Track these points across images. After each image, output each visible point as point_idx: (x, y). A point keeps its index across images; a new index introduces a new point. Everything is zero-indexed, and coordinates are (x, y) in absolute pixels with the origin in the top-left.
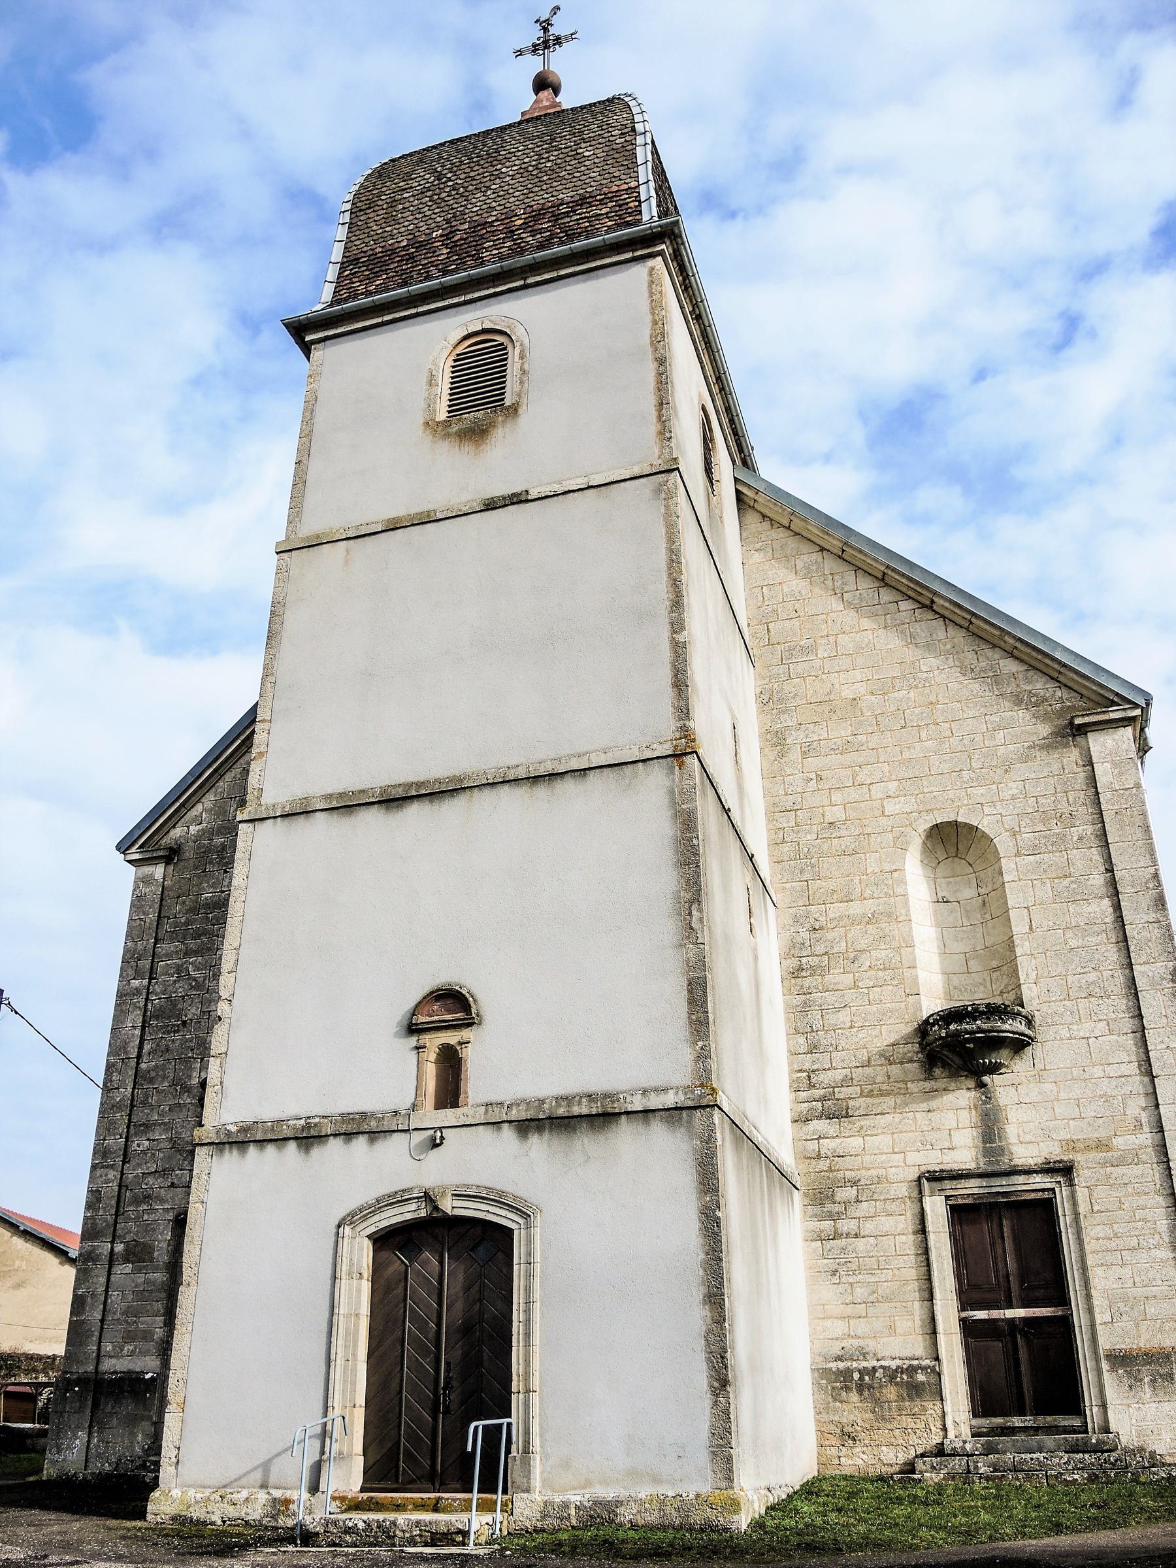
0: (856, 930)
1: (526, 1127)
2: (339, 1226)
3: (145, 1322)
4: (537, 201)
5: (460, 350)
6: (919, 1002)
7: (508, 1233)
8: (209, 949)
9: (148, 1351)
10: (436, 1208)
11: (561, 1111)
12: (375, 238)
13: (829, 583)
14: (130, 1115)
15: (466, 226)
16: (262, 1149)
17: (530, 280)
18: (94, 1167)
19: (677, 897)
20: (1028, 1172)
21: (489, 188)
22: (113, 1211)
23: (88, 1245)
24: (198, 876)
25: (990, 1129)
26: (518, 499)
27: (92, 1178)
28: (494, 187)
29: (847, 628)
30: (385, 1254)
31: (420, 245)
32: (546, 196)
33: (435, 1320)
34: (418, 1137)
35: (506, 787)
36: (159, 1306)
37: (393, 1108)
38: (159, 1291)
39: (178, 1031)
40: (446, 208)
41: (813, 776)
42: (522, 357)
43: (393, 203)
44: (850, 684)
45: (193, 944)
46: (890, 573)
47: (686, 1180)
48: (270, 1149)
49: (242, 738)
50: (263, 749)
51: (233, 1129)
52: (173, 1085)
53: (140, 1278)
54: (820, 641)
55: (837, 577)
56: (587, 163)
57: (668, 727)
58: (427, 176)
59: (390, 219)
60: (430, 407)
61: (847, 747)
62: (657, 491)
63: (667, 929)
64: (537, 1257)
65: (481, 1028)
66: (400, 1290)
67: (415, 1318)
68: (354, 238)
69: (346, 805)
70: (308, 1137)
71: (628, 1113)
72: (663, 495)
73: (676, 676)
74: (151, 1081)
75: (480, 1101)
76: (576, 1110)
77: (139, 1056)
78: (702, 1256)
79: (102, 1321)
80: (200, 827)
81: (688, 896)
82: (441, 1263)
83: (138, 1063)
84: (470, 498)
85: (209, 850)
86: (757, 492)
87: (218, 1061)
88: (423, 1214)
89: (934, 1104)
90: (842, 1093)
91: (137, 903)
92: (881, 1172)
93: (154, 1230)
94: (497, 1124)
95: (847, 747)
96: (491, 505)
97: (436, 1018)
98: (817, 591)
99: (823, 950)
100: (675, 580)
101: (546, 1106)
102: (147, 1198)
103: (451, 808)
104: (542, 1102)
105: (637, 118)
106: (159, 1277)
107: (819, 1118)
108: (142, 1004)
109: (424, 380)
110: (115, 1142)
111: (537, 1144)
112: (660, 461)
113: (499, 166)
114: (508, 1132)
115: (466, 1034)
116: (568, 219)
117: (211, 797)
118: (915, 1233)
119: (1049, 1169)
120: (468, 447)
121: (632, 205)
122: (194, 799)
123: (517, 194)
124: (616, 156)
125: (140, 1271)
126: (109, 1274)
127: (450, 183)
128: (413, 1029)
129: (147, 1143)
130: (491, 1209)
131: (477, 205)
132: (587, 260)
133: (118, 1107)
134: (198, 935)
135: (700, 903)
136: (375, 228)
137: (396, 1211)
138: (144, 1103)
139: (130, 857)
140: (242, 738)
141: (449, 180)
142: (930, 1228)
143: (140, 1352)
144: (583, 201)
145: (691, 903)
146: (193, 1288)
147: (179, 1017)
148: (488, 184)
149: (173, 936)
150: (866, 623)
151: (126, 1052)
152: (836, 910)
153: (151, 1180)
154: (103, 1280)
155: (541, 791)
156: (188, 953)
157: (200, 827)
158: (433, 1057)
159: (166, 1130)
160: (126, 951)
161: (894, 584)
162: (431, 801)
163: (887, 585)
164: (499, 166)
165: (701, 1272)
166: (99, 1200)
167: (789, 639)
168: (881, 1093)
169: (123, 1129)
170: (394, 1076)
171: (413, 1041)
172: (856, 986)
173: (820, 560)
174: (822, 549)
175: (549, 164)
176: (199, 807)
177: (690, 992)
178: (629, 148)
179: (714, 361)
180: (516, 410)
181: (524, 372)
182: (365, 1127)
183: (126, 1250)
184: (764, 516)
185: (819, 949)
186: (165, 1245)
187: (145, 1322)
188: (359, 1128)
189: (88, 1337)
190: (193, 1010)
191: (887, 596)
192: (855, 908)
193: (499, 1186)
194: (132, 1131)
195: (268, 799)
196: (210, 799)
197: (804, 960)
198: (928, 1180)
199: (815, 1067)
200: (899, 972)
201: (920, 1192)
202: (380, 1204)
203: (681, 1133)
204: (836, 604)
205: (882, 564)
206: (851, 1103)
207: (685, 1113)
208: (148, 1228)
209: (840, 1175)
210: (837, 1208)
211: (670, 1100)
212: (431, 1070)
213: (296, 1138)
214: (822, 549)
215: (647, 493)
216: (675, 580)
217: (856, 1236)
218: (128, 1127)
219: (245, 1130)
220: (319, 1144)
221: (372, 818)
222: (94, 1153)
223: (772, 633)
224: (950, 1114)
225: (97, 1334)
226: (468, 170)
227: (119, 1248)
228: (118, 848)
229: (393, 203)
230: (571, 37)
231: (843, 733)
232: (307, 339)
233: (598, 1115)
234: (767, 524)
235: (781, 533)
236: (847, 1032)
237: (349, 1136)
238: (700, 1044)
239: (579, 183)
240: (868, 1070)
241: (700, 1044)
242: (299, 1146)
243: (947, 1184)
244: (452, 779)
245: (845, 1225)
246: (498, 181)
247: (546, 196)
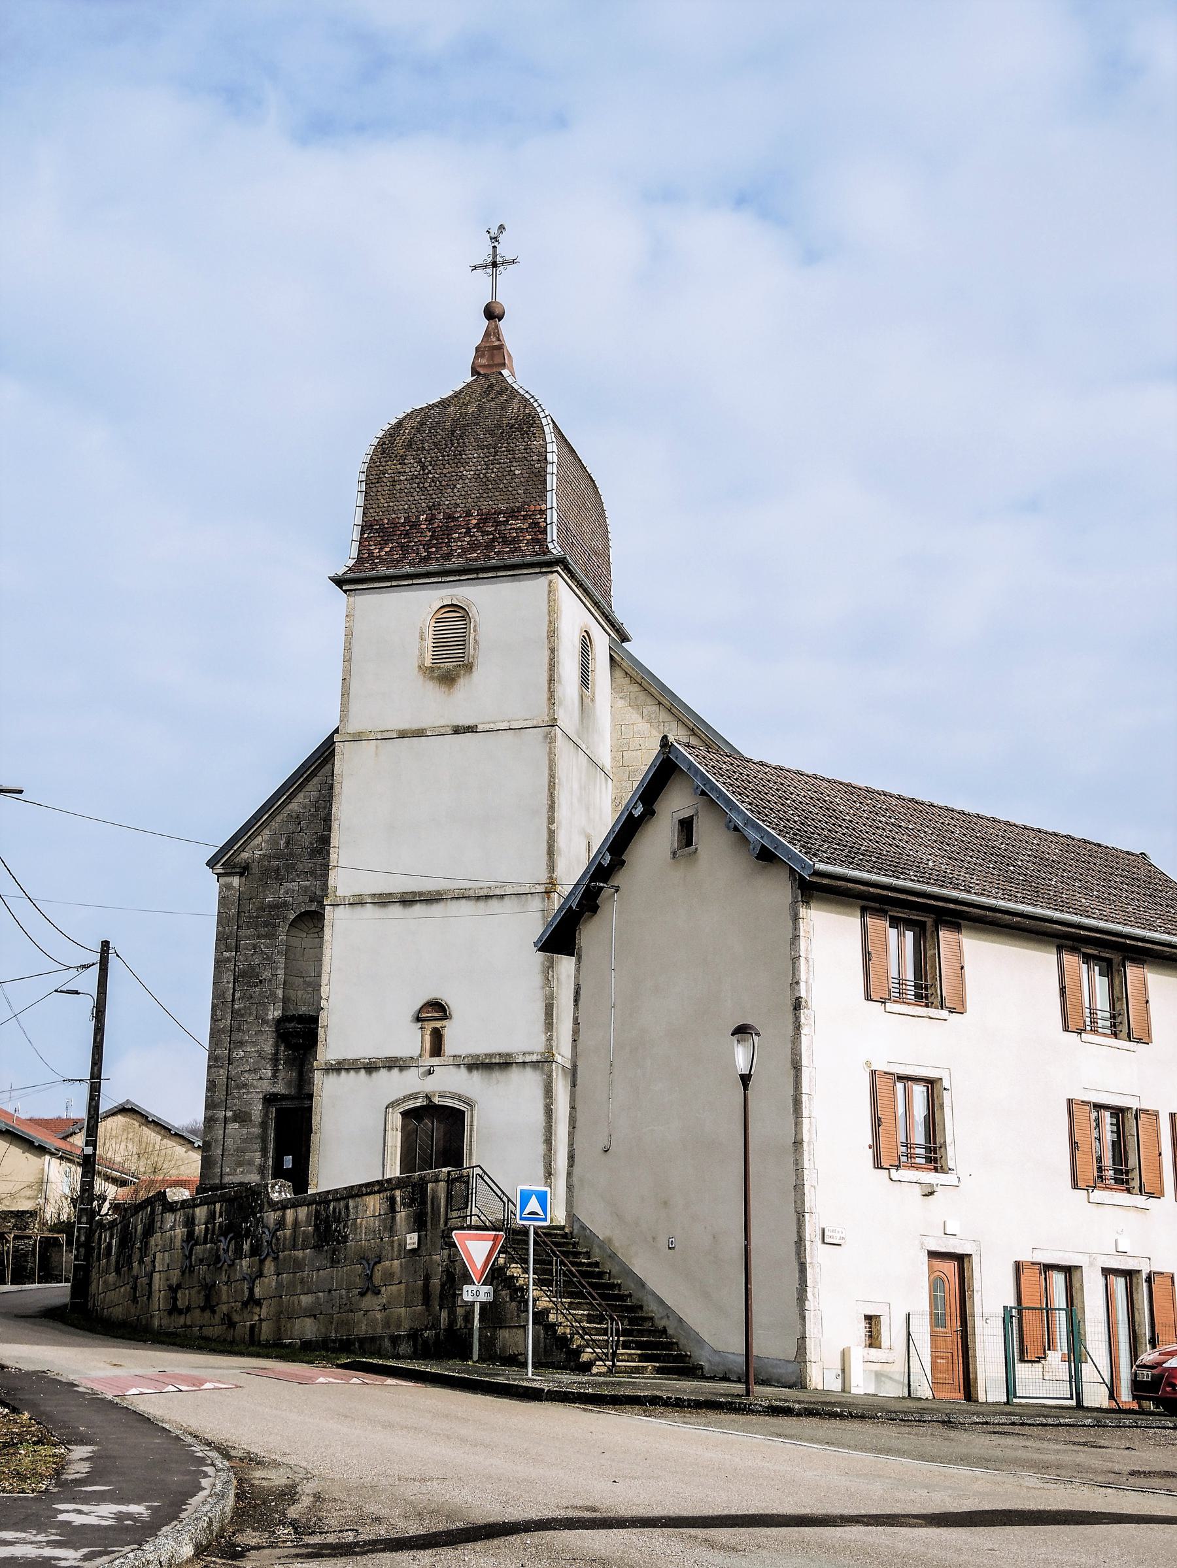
1: (471, 1067)
3: (248, 1156)
13: (661, 728)
17: (480, 576)
18: (209, 1067)
23: (210, 1113)
26: (472, 729)
36: (257, 1147)
45: (263, 931)
47: (539, 1093)
48: (352, 1073)
52: (257, 1018)
53: (245, 1131)
57: (543, 877)
64: (475, 1123)
69: (383, 900)
70: (370, 1068)
74: (242, 1016)
76: (494, 1061)
77: (233, 1000)
91: (223, 902)
96: (457, 731)
102: (245, 1086)
103: (437, 909)
106: (256, 1130)
109: (418, 635)
110: (223, 1052)
111: (476, 1075)
114: (463, 1069)
115: (444, 1023)
120: (444, 689)
128: (418, 1019)
133: (222, 1031)
138: (239, 1029)
149: (249, 925)
154: (221, 1132)
156: (259, 937)
166: (215, 1086)
170: (409, 1041)
174: (660, 703)
176: (260, 838)
187: (248, 1156)
188: (395, 1064)
196: (266, 833)
203: (538, 1072)
208: (248, 1103)
211: (534, 1058)
212: (428, 1038)
214: (660, 703)
215: (540, 737)
219: (339, 1063)
221: (396, 910)
227: (229, 1114)
228: (208, 864)
237: (390, 1068)
244: (438, 892)
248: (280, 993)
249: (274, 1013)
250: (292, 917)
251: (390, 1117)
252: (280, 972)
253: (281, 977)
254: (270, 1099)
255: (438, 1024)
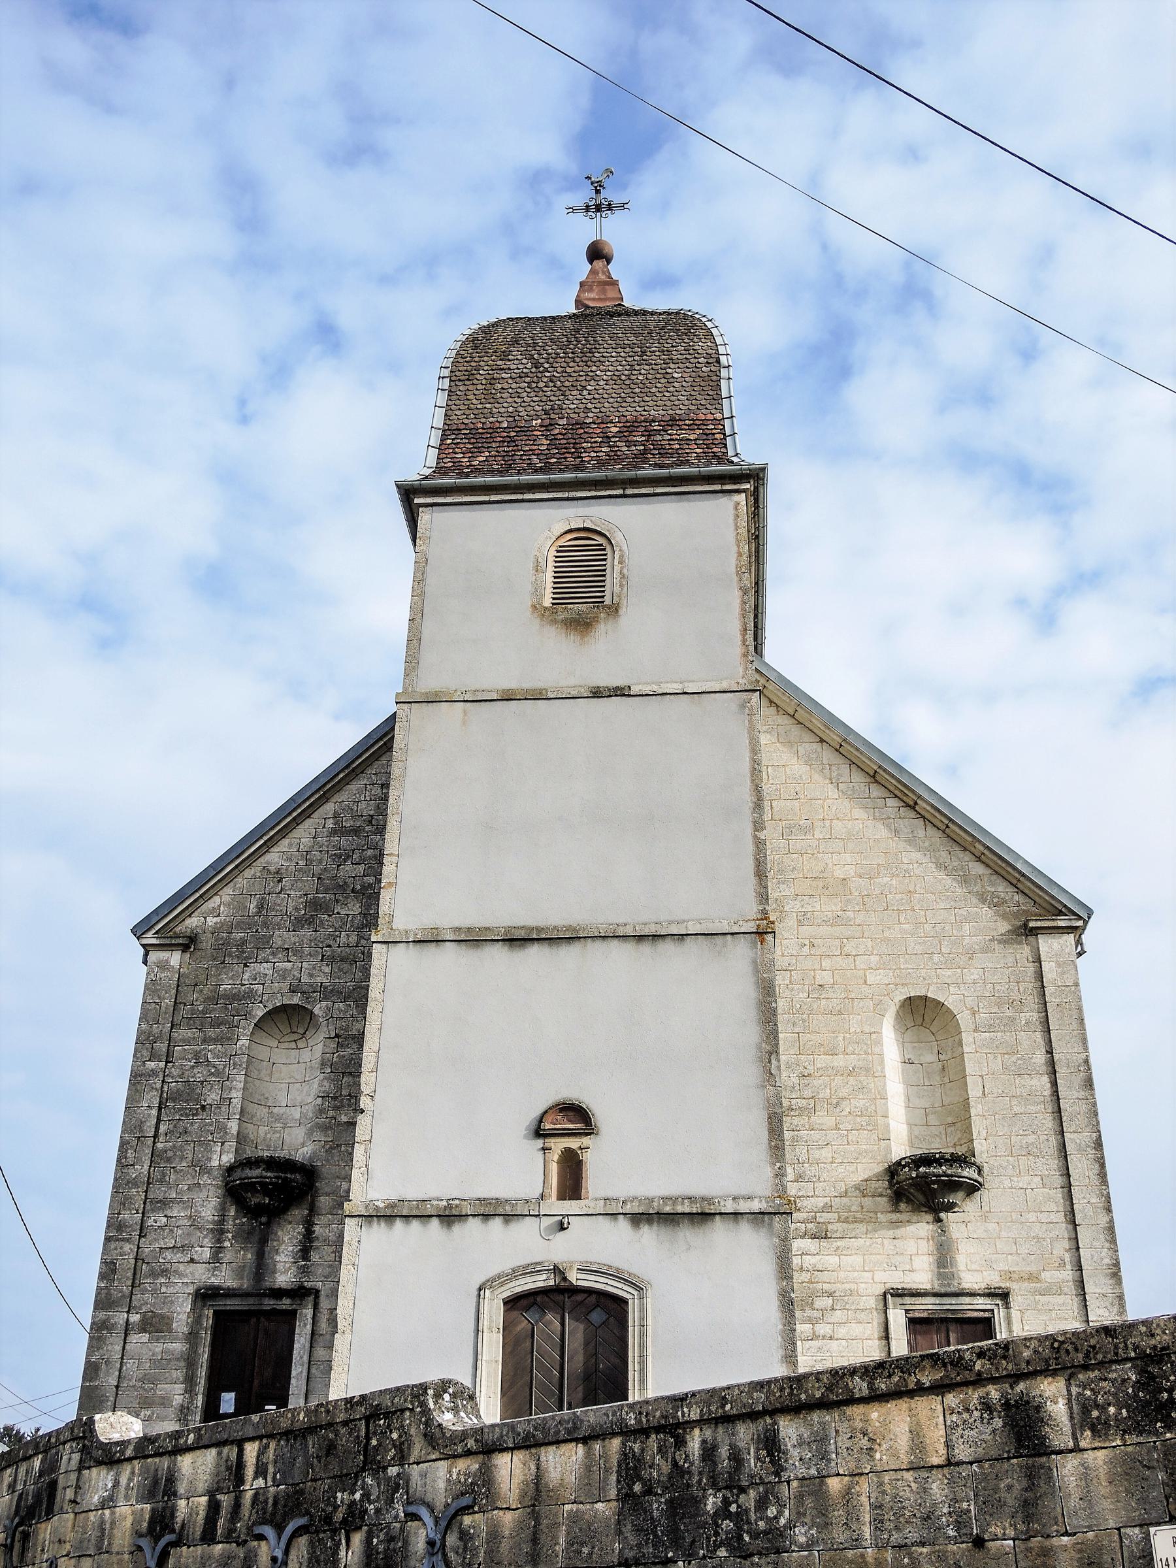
0: (839, 1080)
1: (638, 1219)
2: (480, 1290)
3: (162, 1389)
4: (632, 411)
5: (562, 542)
6: (889, 1146)
7: (622, 1302)
8: (229, 1039)
9: (166, 1417)
10: (565, 1279)
11: (667, 1209)
12: (476, 412)
13: (827, 772)
14: (146, 1192)
15: (564, 421)
16: (408, 1223)
17: (629, 491)
18: (108, 1239)
19: (759, 1047)
20: (973, 1294)
21: (584, 388)
22: (129, 1283)
23: (102, 1315)
24: (217, 967)
25: (944, 1257)
26: (621, 692)
27: (105, 1250)
28: (589, 388)
29: (840, 815)
30: (515, 1314)
31: (522, 431)
32: (638, 409)
33: (558, 1368)
34: (547, 1222)
35: (616, 942)
36: (179, 1374)
37: (524, 1196)
38: (178, 1359)
39: (197, 1115)
40: (544, 399)
41: (807, 942)
42: (621, 562)
43: (492, 381)
44: (842, 865)
45: (212, 1033)
46: (881, 772)
47: (767, 1268)
48: (415, 1224)
49: (265, 838)
50: (392, 879)
51: (382, 1205)
52: (193, 1165)
53: (158, 1348)
54: (817, 824)
55: (833, 768)
56: (676, 384)
57: (752, 909)
58: (524, 361)
59: (489, 396)
60: (537, 591)
61: (837, 920)
62: (742, 706)
63: (752, 1073)
64: (649, 1321)
65: (598, 1138)
66: (528, 1344)
67: (541, 1365)
68: (453, 407)
70: (450, 1216)
71: (721, 1214)
72: (747, 711)
73: (758, 866)
74: (168, 1160)
75: (598, 1196)
76: (680, 1209)
77: (155, 1136)
78: (780, 1327)
79: (117, 1387)
80: (218, 919)
81: (768, 1048)
82: (563, 1324)
83: (154, 1143)
84: (577, 683)
85: (227, 942)
86: (768, 680)
87: (363, 1147)
88: (552, 1283)
89: (899, 1232)
90: (823, 1217)
91: (152, 987)
92: (854, 1286)
93: (172, 1302)
94: (614, 1215)
95: (837, 920)
96: (597, 694)
97: (558, 1126)
98: (817, 777)
99: (811, 1095)
100: (757, 786)
101: (655, 1204)
102: (165, 1272)
103: (568, 954)
104: (652, 1200)
105: (721, 350)
106: (179, 1347)
107: (803, 1237)
108: (159, 1085)
109: (531, 565)
110: (131, 1217)
111: (648, 1234)
112: (745, 681)
113: (594, 368)
114: (623, 1223)
115: (585, 1141)
116: (659, 438)
117: (229, 890)
118: (880, 1339)
119: (990, 1294)
120: (573, 637)
121: (717, 436)
122: (212, 892)
123: (611, 400)
124: (702, 384)
125: (157, 1340)
126: (125, 1343)
127: (547, 374)
128: (539, 1133)
129: (165, 1219)
130: (610, 1282)
131: (573, 403)
132: (681, 484)
133: (135, 1183)
134: (217, 1023)
135: (777, 1054)
136: (474, 401)
137: (528, 1280)
138: (162, 1181)
139: (145, 942)
140: (265, 838)
141: (546, 370)
142: (892, 1335)
143: (158, 1417)
144: (673, 421)
145: (770, 1054)
146: (348, 1335)
147: (198, 1101)
148: (584, 383)
149: (190, 1022)
150: (859, 813)
151: (141, 1131)
152: (822, 1061)
153: (169, 1255)
154: (118, 1348)
155: (646, 948)
156: (204, 1041)
157: (218, 919)
158: (556, 1158)
159: (185, 1208)
160: (140, 1033)
161: (883, 782)
162: (550, 945)
163: (877, 782)
164: (594, 368)
165: (780, 1339)
166: (114, 1271)
167: (789, 817)
168: (856, 1220)
169: (139, 1204)
170: (526, 1172)
171: (540, 1143)
172: (837, 1128)
173: (819, 750)
174: (822, 741)
175: (640, 377)
176: (217, 899)
177: (770, 1124)
178: (714, 378)
179: (757, 570)
180: (617, 610)
181: (623, 577)
182: (500, 1211)
183: (142, 1320)
184: (771, 702)
185: (807, 1093)
186: (184, 1317)
187: (162, 1389)
188: (494, 1211)
189: (102, 1402)
190: (213, 1096)
191: (876, 791)
192: (839, 1061)
193: (616, 1264)
194: (148, 1207)
195: (399, 924)
196: (227, 893)
197: (794, 1101)
198: (892, 1295)
199: (800, 1194)
200: (874, 1119)
201: (885, 1305)
202: (516, 1273)
203: (763, 1232)
204: (832, 792)
205: (875, 763)
206: (830, 1227)
207: (766, 1217)
208: (167, 1301)
209: (819, 1286)
210: (815, 1314)
211: (756, 1206)
212: (554, 1168)
213: (439, 1216)
214: (822, 741)
215: (734, 707)
216: (757, 786)
217: (831, 1338)
218: (145, 1203)
219: (392, 1205)
220: (460, 1221)
221: (497, 954)
222: (108, 1227)
223: (775, 809)
224: (912, 1242)
225: (112, 1399)
226: (564, 364)
227: (135, 1318)
228: (134, 931)
229: (492, 381)
230: (623, 206)
231: (834, 908)
232: (417, 501)
233: (697, 1214)
234: (773, 710)
235: (786, 720)
236: (828, 1166)
237: (486, 1217)
238: (778, 1165)
239: (668, 403)
240: (845, 1200)
241: (778, 1165)
242: (442, 1222)
243: (907, 1300)
244: (569, 928)
245: (822, 1329)
246: (592, 383)
247: (638, 409)
248: (233, 1126)
249: (223, 1157)
250: (260, 1013)
251: (486, 1306)
252: (236, 1094)
253: (237, 1103)
254: (205, 1295)
255: (573, 1143)
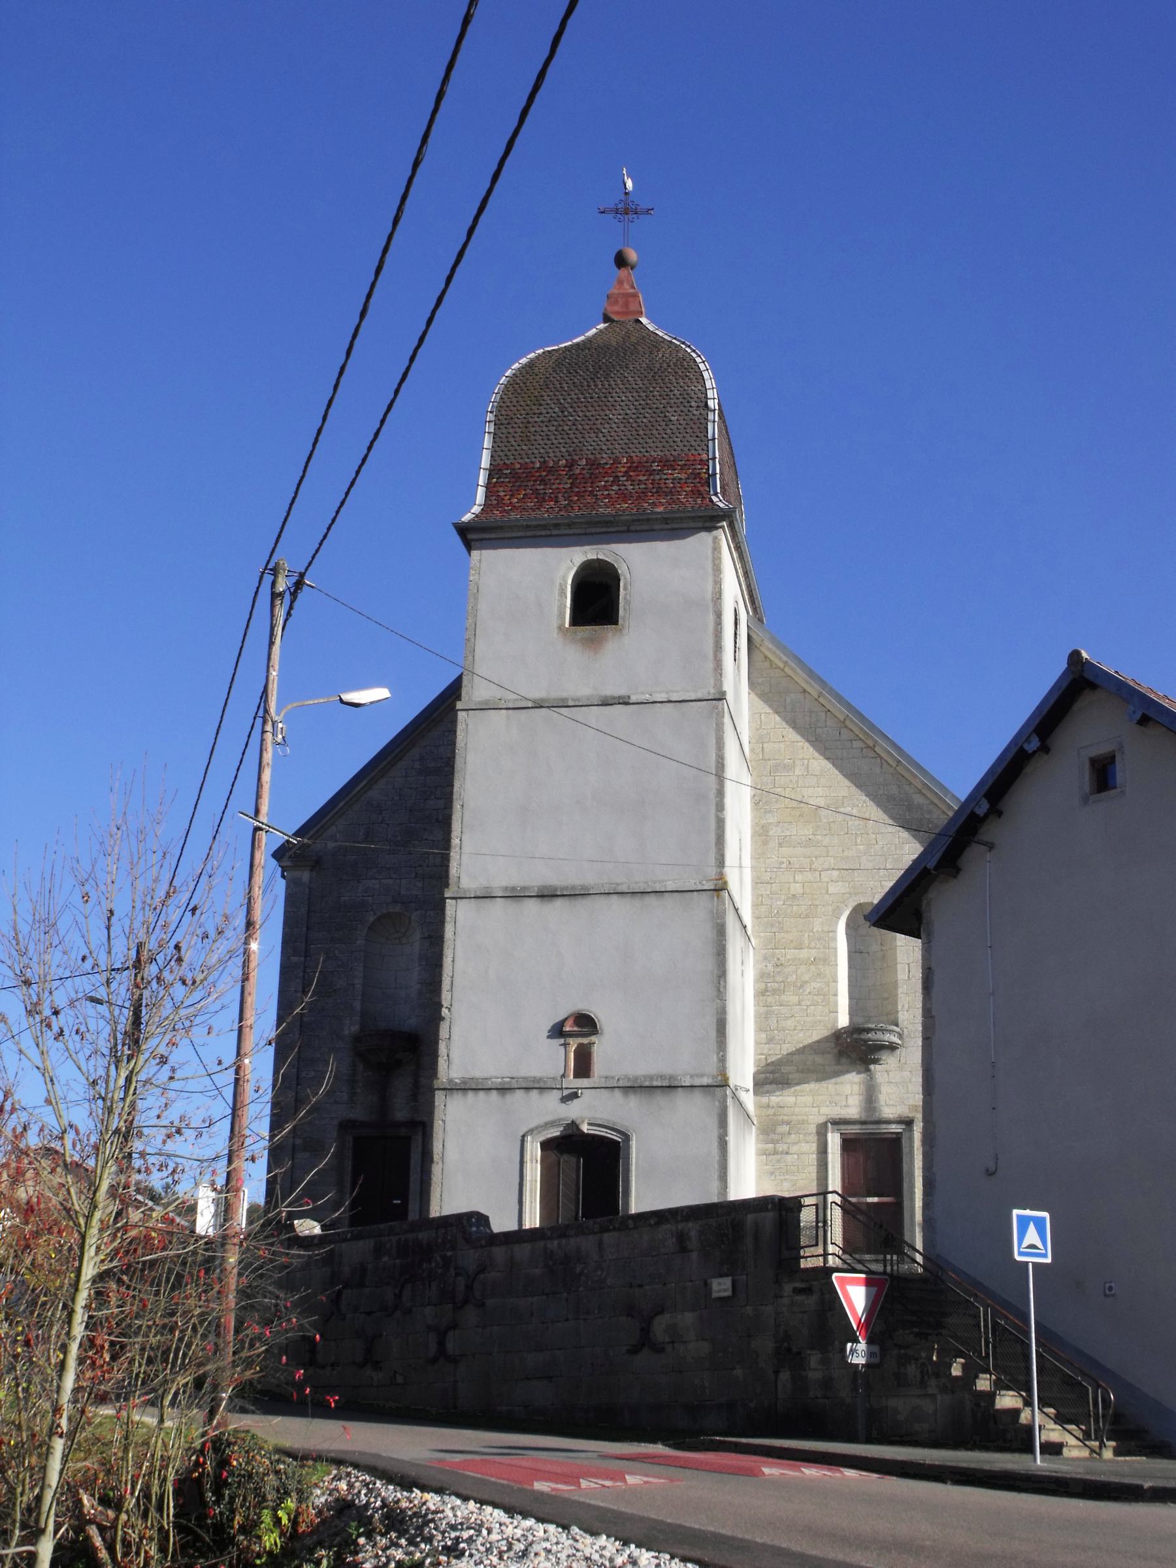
0: (803, 968)
6: (836, 1018)
11: (647, 1084)
20: (889, 1122)
25: (870, 1096)
31: (551, 471)
35: (615, 896)
54: (798, 763)
61: (809, 843)
69: (515, 895)
76: (655, 1084)
89: (839, 1079)
90: (785, 1069)
95: (809, 843)
107: (770, 1083)
108: (301, 974)
111: (634, 1102)
115: (593, 1038)
119: (900, 1121)
129: (313, 1073)
155: (637, 902)
170: (553, 1059)
172: (799, 1004)
176: (334, 828)
182: (537, 1085)
185: (779, 979)
192: (804, 954)
200: (827, 996)
211: (705, 1081)
219: (464, 1081)
221: (532, 905)
223: (766, 750)
224: (848, 1086)
243: (842, 1127)
244: (583, 887)
248: (357, 1005)
249: (351, 1028)
250: (372, 919)
251: (528, 1146)
252: (358, 982)
253: (359, 987)
254: (346, 1126)
255: (585, 1041)
